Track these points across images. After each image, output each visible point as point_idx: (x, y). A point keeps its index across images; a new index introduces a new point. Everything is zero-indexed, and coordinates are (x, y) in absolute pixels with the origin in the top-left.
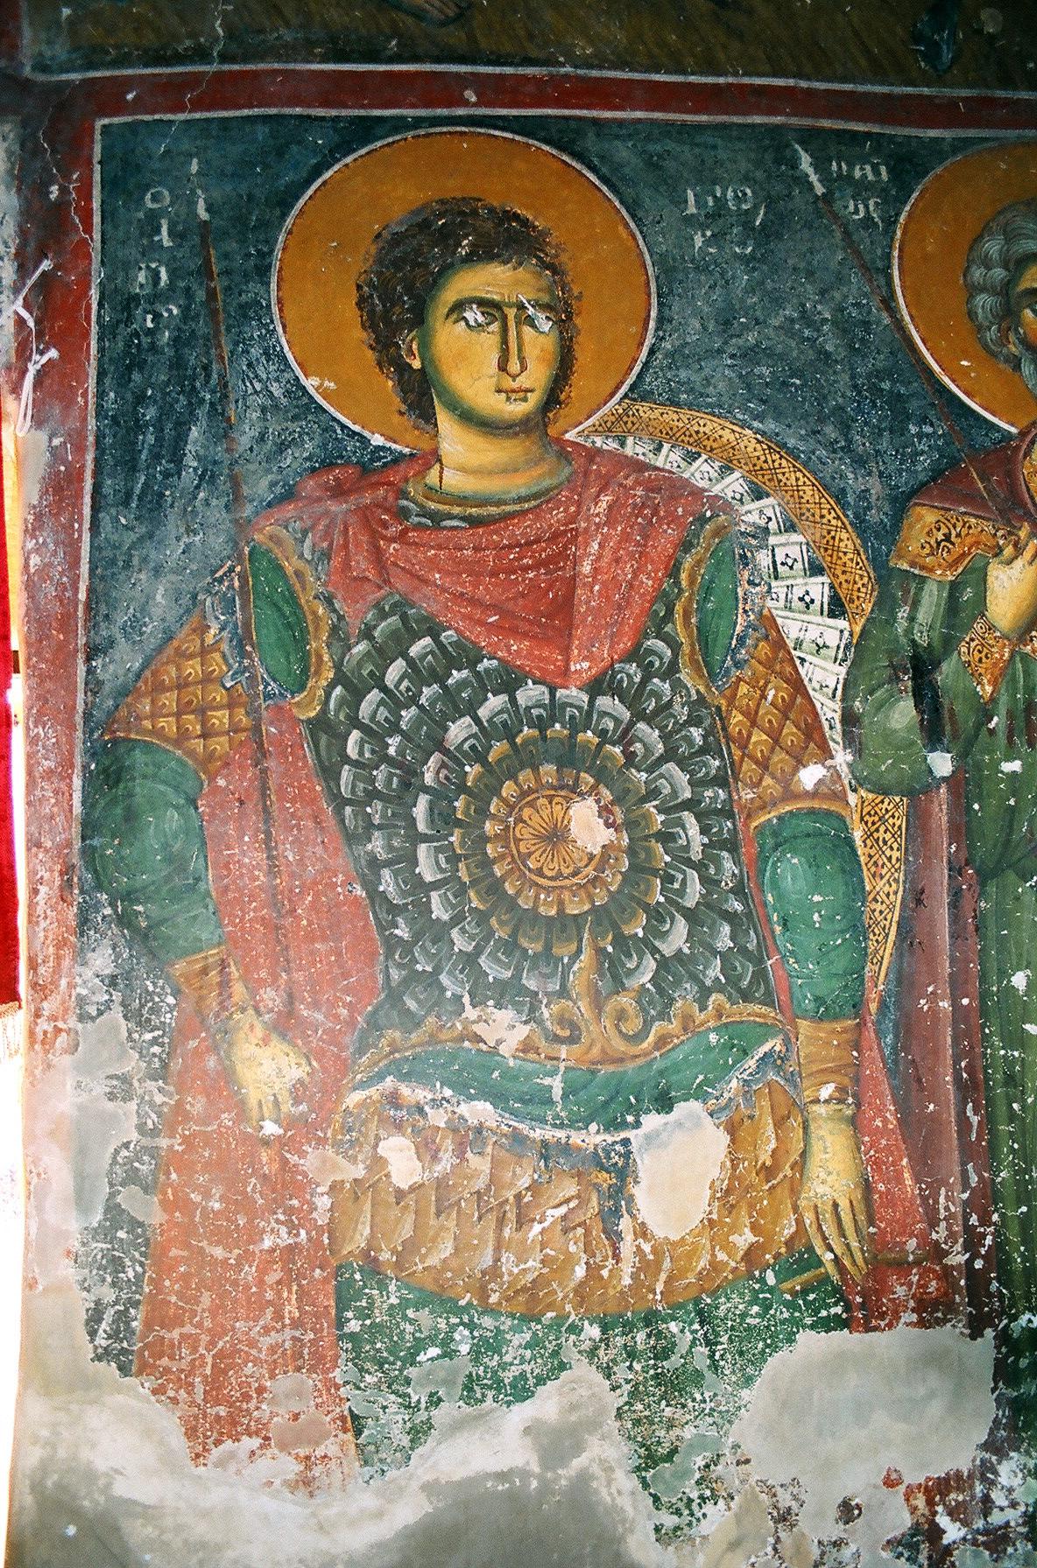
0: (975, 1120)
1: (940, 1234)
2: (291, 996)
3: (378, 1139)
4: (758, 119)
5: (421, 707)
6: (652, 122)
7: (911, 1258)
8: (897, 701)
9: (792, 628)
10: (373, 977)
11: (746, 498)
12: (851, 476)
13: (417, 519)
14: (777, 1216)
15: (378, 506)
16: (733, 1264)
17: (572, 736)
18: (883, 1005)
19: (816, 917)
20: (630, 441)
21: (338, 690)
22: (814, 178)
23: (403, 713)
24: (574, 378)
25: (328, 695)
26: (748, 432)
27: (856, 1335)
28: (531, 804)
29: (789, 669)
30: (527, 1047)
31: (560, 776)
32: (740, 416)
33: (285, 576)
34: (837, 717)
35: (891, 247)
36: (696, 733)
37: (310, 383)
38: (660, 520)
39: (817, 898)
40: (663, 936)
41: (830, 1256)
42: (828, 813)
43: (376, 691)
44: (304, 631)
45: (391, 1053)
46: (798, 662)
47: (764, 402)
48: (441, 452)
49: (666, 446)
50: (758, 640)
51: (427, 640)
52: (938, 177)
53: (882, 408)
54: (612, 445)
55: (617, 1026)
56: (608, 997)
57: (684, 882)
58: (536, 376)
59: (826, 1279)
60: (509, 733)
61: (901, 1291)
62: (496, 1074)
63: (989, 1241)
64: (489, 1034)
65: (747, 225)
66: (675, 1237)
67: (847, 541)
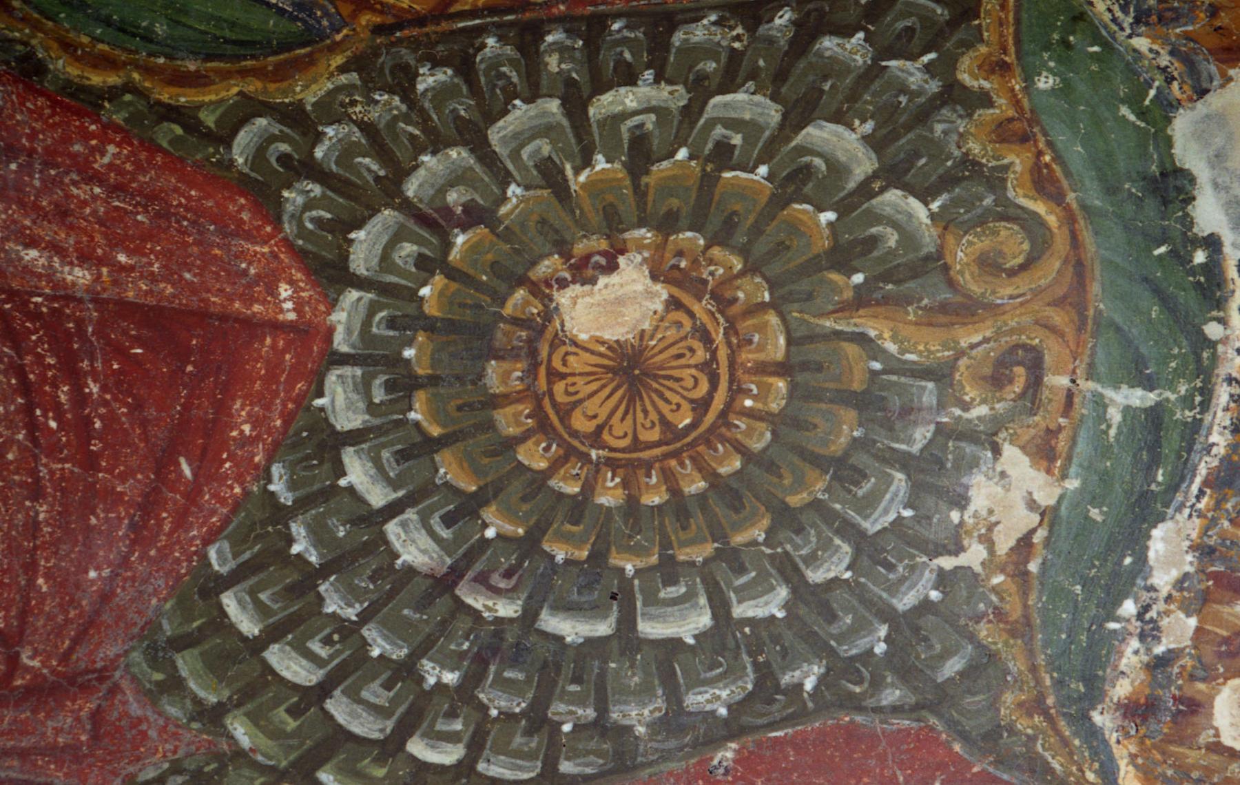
3: (1216, 747)
5: (364, 618)
17: (430, 326)
23: (376, 653)
28: (565, 413)
30: (1044, 453)
36: (428, 80)
40: (837, 170)
43: (330, 705)
45: (1045, 713)
51: (229, 602)
55: (1012, 273)
56: (951, 284)
60: (421, 448)
62: (1095, 513)
64: (1021, 520)
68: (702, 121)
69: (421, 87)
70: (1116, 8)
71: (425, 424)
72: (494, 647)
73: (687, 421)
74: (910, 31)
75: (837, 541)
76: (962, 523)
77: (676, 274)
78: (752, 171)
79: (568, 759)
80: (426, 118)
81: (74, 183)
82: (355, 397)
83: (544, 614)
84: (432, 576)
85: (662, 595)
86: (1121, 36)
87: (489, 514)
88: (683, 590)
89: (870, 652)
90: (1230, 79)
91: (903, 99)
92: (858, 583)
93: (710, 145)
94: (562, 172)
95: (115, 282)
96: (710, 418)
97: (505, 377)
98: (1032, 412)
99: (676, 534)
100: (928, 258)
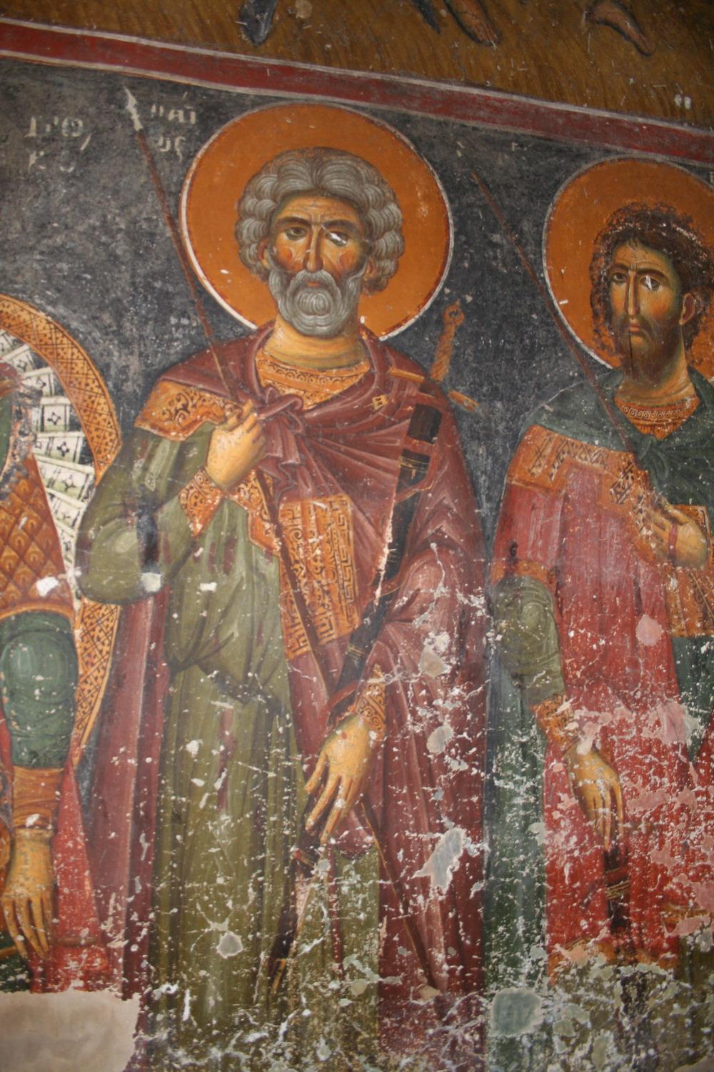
0: (146, 846)
1: (107, 926)
4: (100, 66)
6: (15, 60)
7: (83, 942)
8: (124, 531)
9: (48, 470)
12: (116, 354)
18: (83, 760)
19: (37, 692)
22: (135, 117)
26: (42, 314)
27: (35, 995)
29: (40, 502)
32: (38, 301)
34: (73, 542)
35: (185, 176)
39: (39, 678)
41: (20, 938)
42: (57, 615)
47: (59, 291)
50: (20, 478)
52: (236, 125)
53: (151, 303)
59: (16, 954)
61: (73, 965)
63: (144, 932)
65: (74, 150)
67: (104, 405)
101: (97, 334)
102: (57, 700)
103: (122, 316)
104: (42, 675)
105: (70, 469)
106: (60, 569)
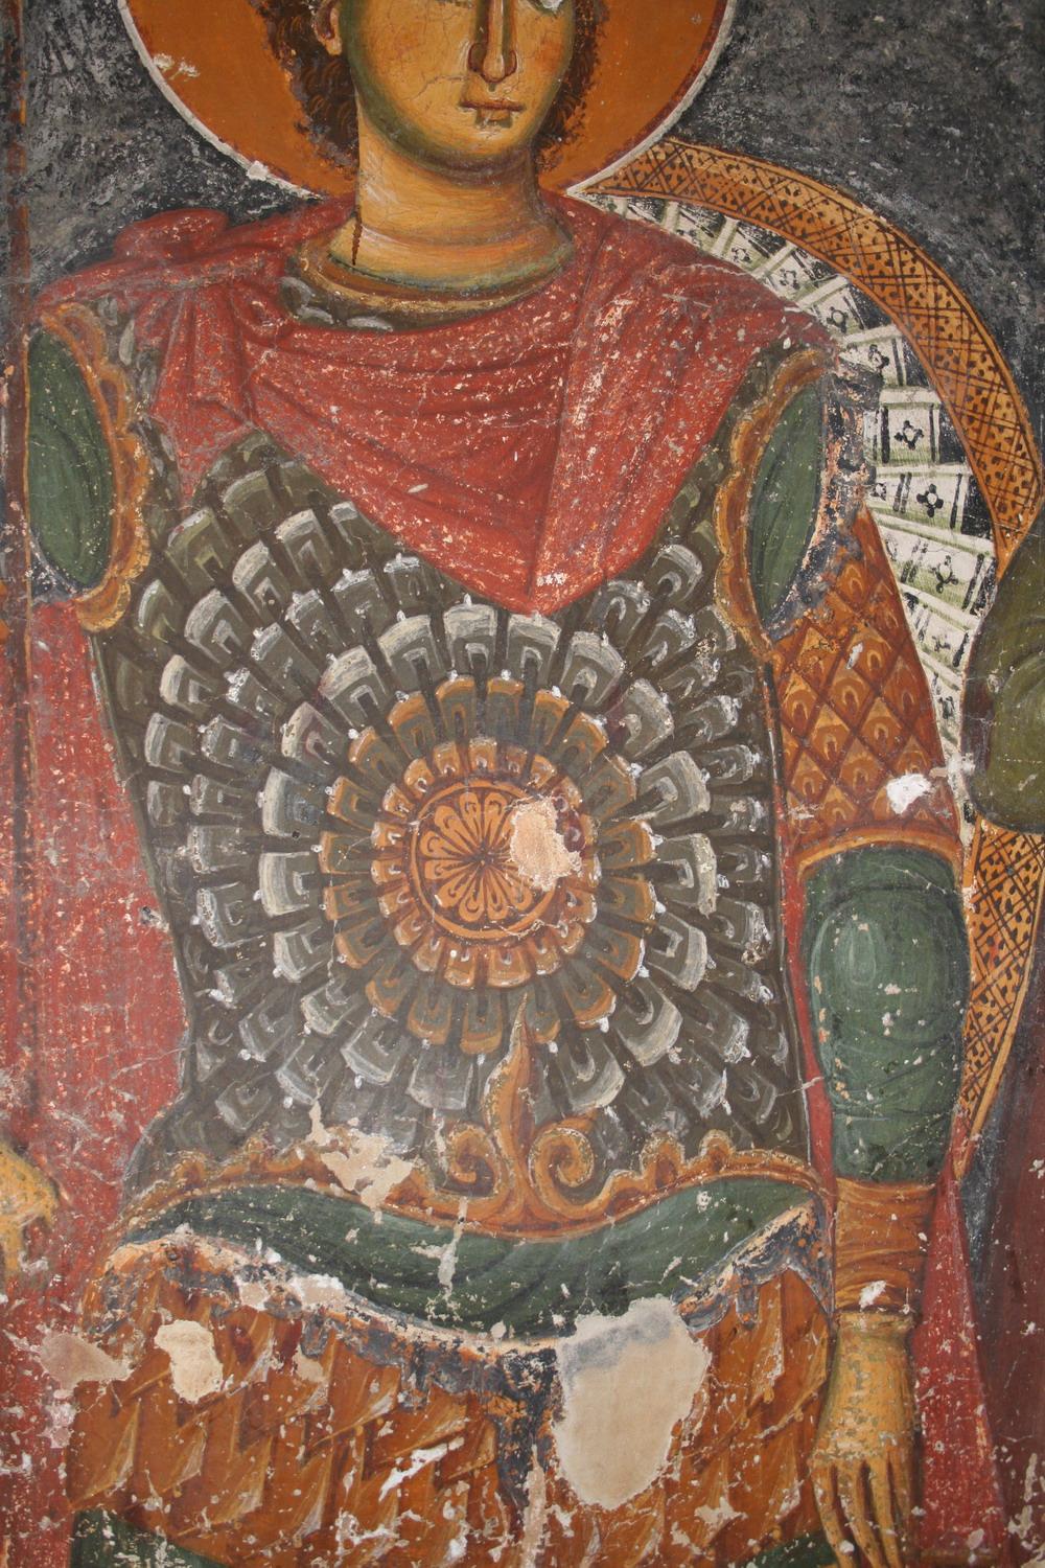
2: (35, 1085)
3: (157, 1322)
5: (287, 626)
9: (901, 545)
10: (169, 1063)
11: (852, 323)
13: (309, 311)
14: (772, 1482)
15: (247, 283)
16: (696, 1551)
17: (527, 695)
19: (886, 1019)
20: (672, 209)
21: (155, 588)
23: (257, 634)
24: (591, 94)
25: (137, 593)
26: (867, 211)
28: (451, 801)
29: (889, 613)
30: (405, 1195)
31: (501, 761)
32: (856, 183)
33: (85, 391)
34: (957, 696)
36: (729, 706)
37: (157, 65)
38: (706, 349)
40: (642, 1032)
41: (847, 1547)
42: (926, 853)
43: (215, 594)
44: (108, 484)
45: (189, 1187)
46: (905, 602)
47: (898, 162)
48: (361, 202)
49: (730, 224)
51: (306, 516)
54: (641, 213)
55: (552, 1173)
56: (545, 1124)
57: (683, 947)
58: (528, 85)
60: (426, 678)
62: (352, 1234)
64: (349, 1174)
66: (610, 1504)
67: (1006, 408)
68: (686, 925)
69: (723, 699)
70: (757, 1253)
71: (446, 684)
72: (257, 731)
73: (440, 903)
74: (750, 1093)
75: (336, 1023)
76: (349, 1127)
77: (564, 898)
78: (644, 964)
79: (161, 789)
80: (698, 701)
81: (654, 419)
82: (471, 629)
83: (283, 775)
84: (319, 684)
85: (296, 874)
86: (735, 1258)
87: (369, 733)
88: (299, 893)
89: (242, 1046)
90: (696, 1340)
91: (695, 1087)
92: (299, 1039)
93: (666, 931)
94: (650, 809)
95: (573, 444)
96: (444, 922)
97: (482, 753)
98: (438, 1185)
99: (347, 889)
100: (568, 1106)
101: (983, 256)
102: (927, 1037)
103: (1031, 218)
104: (898, 983)
105: (945, 543)
106: (932, 757)
